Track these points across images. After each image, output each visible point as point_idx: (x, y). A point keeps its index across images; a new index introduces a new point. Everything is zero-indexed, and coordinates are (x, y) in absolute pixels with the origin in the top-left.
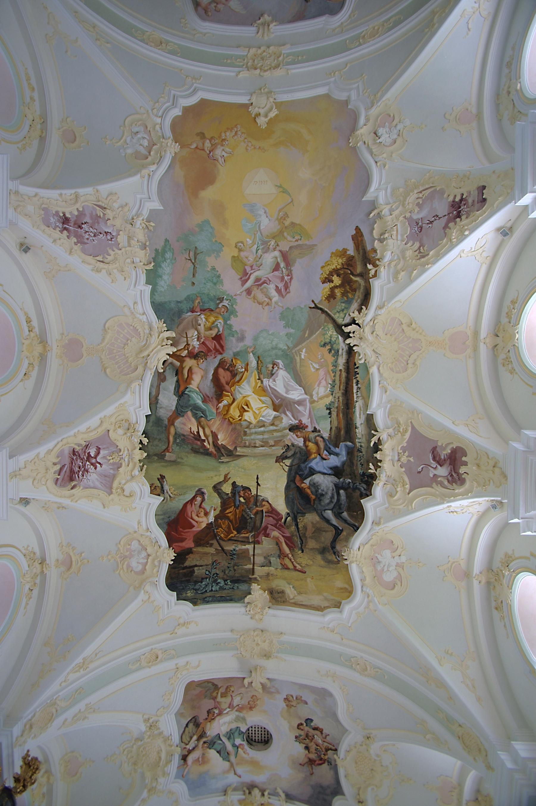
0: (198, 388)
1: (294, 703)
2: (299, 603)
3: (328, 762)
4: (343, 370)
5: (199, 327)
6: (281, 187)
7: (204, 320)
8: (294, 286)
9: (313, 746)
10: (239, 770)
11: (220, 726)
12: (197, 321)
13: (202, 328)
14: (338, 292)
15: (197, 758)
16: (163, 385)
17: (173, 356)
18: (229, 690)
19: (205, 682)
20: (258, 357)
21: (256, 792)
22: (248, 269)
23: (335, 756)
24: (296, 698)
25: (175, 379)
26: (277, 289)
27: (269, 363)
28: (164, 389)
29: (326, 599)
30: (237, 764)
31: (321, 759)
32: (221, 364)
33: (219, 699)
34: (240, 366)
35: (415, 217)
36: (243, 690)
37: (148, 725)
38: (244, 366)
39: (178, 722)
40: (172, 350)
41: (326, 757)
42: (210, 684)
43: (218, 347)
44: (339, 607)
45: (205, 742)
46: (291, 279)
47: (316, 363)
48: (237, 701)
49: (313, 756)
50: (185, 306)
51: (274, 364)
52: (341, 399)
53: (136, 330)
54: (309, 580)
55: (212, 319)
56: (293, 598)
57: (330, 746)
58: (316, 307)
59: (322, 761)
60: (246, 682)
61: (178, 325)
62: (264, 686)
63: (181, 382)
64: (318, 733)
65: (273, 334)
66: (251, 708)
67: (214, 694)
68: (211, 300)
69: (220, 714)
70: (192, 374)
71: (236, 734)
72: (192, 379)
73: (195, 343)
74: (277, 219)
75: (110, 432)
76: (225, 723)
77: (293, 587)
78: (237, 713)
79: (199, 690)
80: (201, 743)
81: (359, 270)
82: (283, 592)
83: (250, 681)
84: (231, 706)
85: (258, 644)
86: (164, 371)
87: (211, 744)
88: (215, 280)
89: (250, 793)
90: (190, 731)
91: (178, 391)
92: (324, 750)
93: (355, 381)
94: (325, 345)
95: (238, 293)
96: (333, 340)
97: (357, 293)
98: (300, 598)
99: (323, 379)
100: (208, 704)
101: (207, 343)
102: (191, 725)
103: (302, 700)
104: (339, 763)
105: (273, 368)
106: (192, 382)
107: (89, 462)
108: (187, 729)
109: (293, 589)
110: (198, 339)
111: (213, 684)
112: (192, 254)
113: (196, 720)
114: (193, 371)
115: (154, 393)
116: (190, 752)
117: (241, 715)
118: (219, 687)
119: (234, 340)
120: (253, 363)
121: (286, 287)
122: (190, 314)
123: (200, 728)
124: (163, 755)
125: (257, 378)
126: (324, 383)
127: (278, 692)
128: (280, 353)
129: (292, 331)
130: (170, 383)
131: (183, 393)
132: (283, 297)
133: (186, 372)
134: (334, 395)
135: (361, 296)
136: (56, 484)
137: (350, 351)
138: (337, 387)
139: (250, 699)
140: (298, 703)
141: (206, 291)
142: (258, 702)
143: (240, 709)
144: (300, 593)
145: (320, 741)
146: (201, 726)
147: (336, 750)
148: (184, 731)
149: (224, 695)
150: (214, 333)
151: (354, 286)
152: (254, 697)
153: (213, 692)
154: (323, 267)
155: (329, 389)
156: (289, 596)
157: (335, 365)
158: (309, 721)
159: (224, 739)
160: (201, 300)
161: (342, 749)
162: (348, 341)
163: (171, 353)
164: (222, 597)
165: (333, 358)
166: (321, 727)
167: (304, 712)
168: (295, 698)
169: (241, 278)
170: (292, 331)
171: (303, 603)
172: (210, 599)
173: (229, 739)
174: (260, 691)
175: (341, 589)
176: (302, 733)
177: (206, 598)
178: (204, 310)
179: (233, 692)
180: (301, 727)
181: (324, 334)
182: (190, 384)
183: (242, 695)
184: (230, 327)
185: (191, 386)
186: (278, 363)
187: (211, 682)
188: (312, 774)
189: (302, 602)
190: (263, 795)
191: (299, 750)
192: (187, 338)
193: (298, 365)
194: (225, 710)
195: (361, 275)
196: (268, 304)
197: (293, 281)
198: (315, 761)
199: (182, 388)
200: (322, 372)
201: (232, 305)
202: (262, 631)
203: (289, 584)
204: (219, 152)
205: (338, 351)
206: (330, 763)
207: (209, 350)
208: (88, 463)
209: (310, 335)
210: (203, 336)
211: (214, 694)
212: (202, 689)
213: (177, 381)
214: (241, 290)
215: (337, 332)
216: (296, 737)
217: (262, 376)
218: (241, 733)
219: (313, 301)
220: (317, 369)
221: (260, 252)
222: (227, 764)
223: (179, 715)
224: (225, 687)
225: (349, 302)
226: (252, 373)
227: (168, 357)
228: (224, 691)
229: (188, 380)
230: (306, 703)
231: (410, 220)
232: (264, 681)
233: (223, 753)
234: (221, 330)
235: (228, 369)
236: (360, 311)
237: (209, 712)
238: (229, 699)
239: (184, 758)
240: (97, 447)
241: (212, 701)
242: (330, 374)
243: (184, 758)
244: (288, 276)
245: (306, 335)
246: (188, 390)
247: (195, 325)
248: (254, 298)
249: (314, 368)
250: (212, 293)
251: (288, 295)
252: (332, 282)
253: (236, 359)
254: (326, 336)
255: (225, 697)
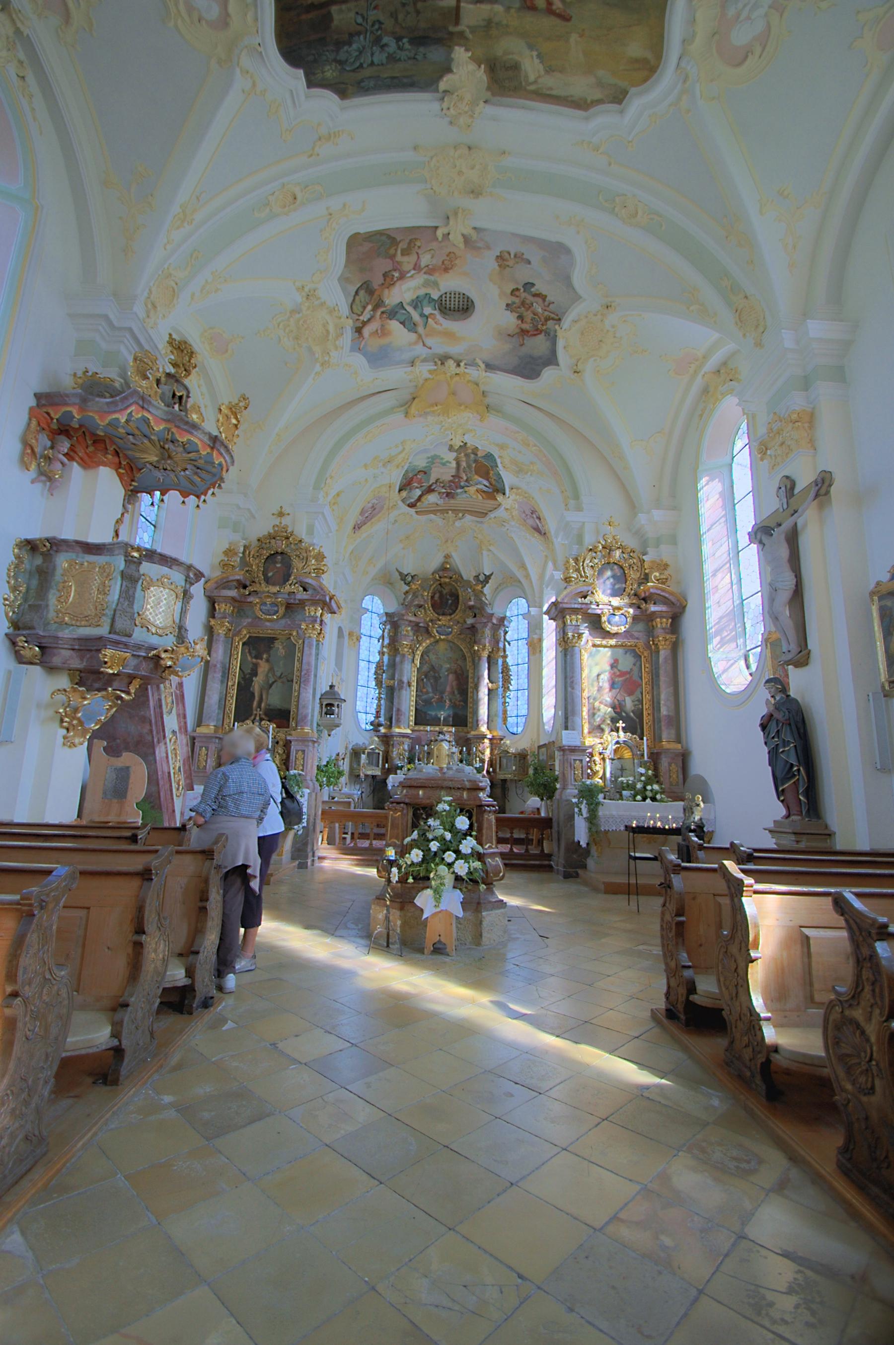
1: (510, 263)
2: (545, 91)
3: (546, 332)
9: (528, 315)
10: (429, 341)
11: (403, 292)
15: (375, 329)
18: (412, 245)
19: (375, 235)
21: (451, 363)
23: (557, 327)
24: (515, 256)
29: (600, 84)
30: (427, 336)
31: (537, 330)
33: (399, 257)
36: (434, 245)
37: (304, 294)
39: (344, 290)
41: (545, 327)
42: (384, 238)
44: (620, 102)
45: (383, 313)
48: (425, 260)
49: (526, 326)
54: (574, 37)
56: (535, 82)
57: (553, 316)
59: (538, 332)
60: (439, 233)
62: (467, 239)
64: (540, 300)
66: (446, 270)
67: (392, 251)
69: (402, 277)
71: (425, 302)
76: (409, 289)
77: (539, 56)
78: (426, 276)
79: (367, 246)
80: (379, 313)
82: (515, 67)
83: (446, 231)
84: (417, 267)
85: (460, 173)
87: (392, 314)
89: (442, 364)
90: (363, 300)
92: (543, 320)
98: (550, 82)
100: (382, 265)
102: (362, 293)
103: (523, 259)
104: (560, 334)
108: (357, 298)
109: (537, 61)
111: (389, 237)
113: (368, 286)
116: (365, 323)
117: (432, 278)
118: (398, 240)
123: (375, 296)
124: (331, 328)
127: (488, 248)
139: (445, 257)
140: (517, 263)
142: (457, 262)
143: (430, 271)
144: (549, 70)
145: (540, 310)
146: (377, 293)
147: (560, 320)
148: (354, 300)
149: (406, 252)
152: (452, 255)
153: (389, 248)
156: (526, 77)
158: (528, 285)
159: (410, 309)
161: (566, 322)
164: (393, 78)
166: (544, 293)
167: (523, 274)
168: (512, 256)
171: (554, 93)
172: (372, 83)
173: (415, 308)
174: (462, 246)
175: (637, 61)
176: (517, 300)
177: (362, 81)
179: (419, 247)
180: (517, 293)
183: (432, 252)
187: (384, 234)
188: (522, 345)
189: (551, 89)
190: (459, 365)
191: (510, 320)
194: (408, 272)
198: (528, 332)
202: (470, 148)
203: (531, 47)
206: (547, 333)
211: (392, 251)
212: (371, 245)
216: (508, 305)
218: (431, 300)
222: (413, 336)
223: (344, 280)
224: (408, 241)
228: (405, 247)
230: (529, 263)
232: (468, 231)
233: (409, 324)
237: (385, 275)
238: (413, 258)
239: (359, 331)
241: (388, 260)
243: (359, 331)
255: (408, 254)
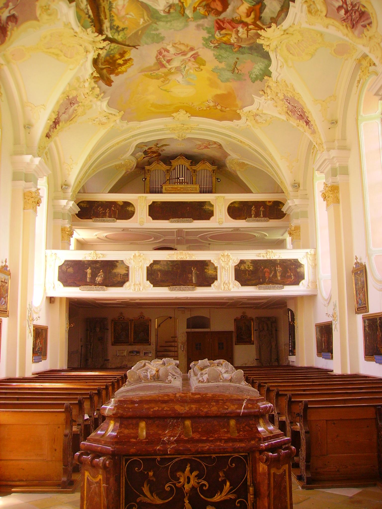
0: (243, 3)
4: (104, 20)
5: (236, 37)
6: (168, 92)
7: (232, 40)
8: (155, 53)
12: (238, 40)
13: (234, 36)
14: (117, 56)
16: (275, 16)
17: (261, 28)
20: (183, 15)
22: (192, 59)
25: (263, 15)
26: (168, 51)
27: (173, 13)
28: (274, 12)
32: (218, 13)
34: (202, 11)
35: (76, 105)
38: (198, 11)
40: (261, 32)
43: (221, 24)
46: (157, 56)
47: (130, 18)
50: (246, 51)
51: (169, 12)
52: (101, 1)
53: (288, 50)
55: (225, 39)
58: (134, 47)
61: (253, 43)
63: (258, 11)
65: (171, 29)
68: (223, 48)
70: (247, 14)
72: (247, 10)
73: (240, 29)
74: (170, 80)
75: (324, 13)
81: (105, 71)
86: (271, 23)
88: (220, 57)
91: (262, 6)
93: (92, 17)
94: (123, 29)
95: (201, 49)
96: (117, 34)
97: (103, 61)
99: (121, 10)
101: (230, 27)
105: (169, 10)
106: (247, 8)
107: (348, 9)
110: (238, 31)
112: (236, 71)
114: (246, 14)
115: (283, 15)
119: (206, 25)
120: (189, 12)
121: (160, 53)
122: (243, 46)
125: (184, 4)
126: (120, 8)
128: (162, 20)
129: (154, 32)
130: (267, 14)
131: (257, 3)
132: (163, 48)
133: (252, 16)
134: (108, 2)
135: (100, 61)
136: (370, 24)
137: (100, 32)
138: (107, 7)
141: (228, 53)
150: (223, 32)
151: (106, 63)
154: (132, 65)
155: (114, 4)
157: (111, 21)
160: (232, 50)
162: (104, 37)
163: (262, 30)
165: (114, 24)
169: (198, 55)
170: (154, 32)
178: (231, 44)
181: (125, 34)
182: (250, 7)
184: (209, 32)
185: (250, 6)
186: (164, 13)
192: (247, 35)
193: (145, 14)
195: (102, 69)
196: (175, 44)
197: (156, 55)
199: (258, 7)
200: (123, 13)
201: (206, 43)
204: (212, 104)
205: (111, 29)
207: (229, 23)
208: (349, 9)
209: (137, 32)
210: (234, 32)
213: (261, 12)
214: (198, 50)
215: (115, 39)
217: (180, 4)
219: (137, 49)
220: (127, 14)
221: (183, 66)
225: (108, 55)
226: (189, 6)
227: (266, 29)
229: (251, 10)
231: (78, 102)
234: (217, 32)
235: (213, 9)
236: (99, 55)
240: (338, 13)
242: (116, 14)
244: (159, 58)
245: (140, 32)
246: (253, 4)
247: (239, 39)
248: (187, 46)
249: (130, 15)
250: (223, 51)
251: (159, 49)
252: (123, 60)
253: (205, 15)
254: (123, 34)
